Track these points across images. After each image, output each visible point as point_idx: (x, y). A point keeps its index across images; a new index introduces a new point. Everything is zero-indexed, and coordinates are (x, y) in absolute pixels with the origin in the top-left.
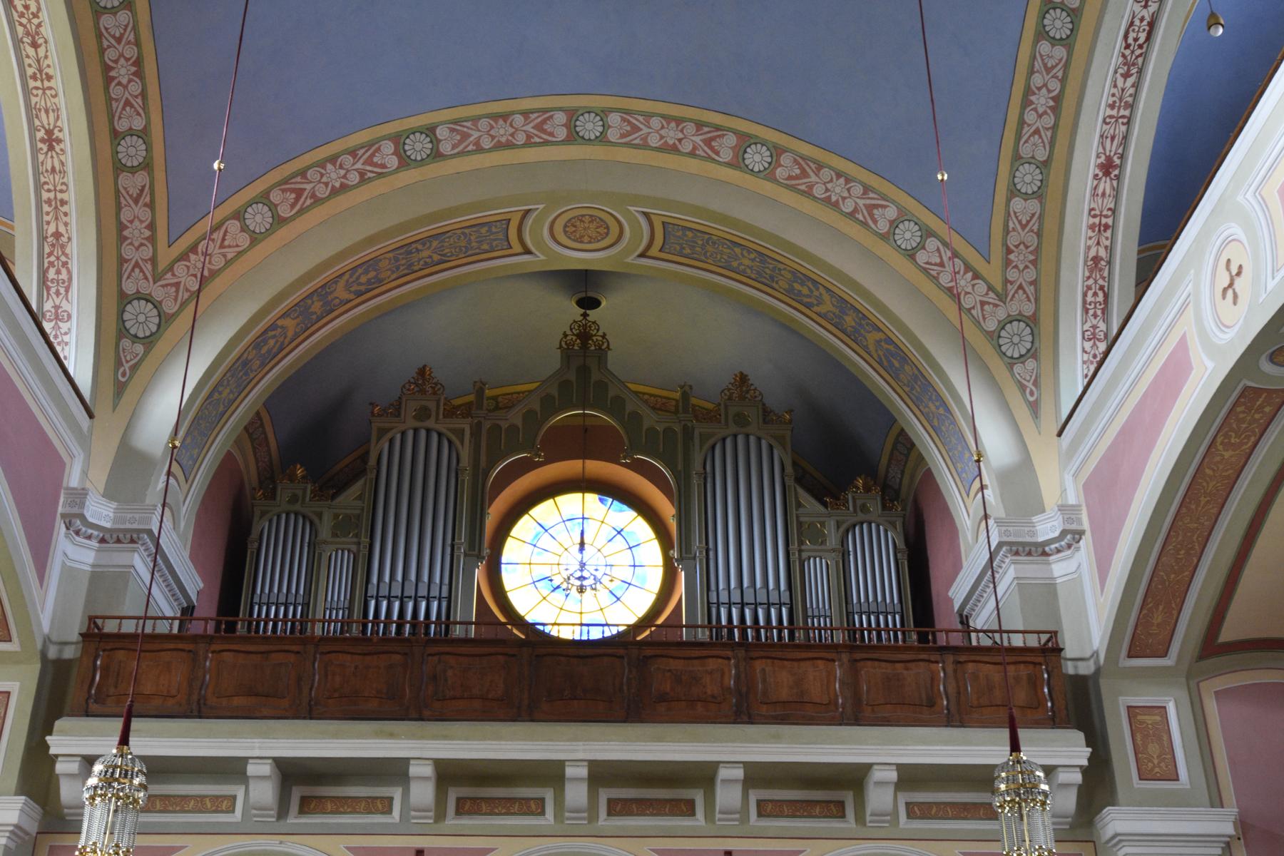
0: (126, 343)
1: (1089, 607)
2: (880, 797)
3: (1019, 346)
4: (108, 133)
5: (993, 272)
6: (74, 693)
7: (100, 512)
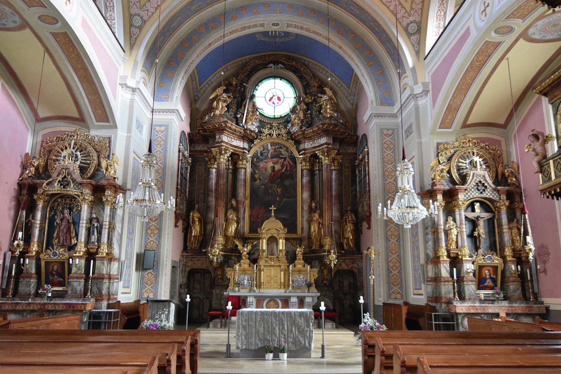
0: (133, 29)
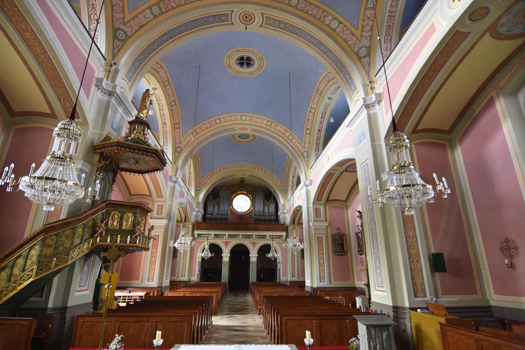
1: (288, 221)
2: (267, 237)
3: (285, 192)
4: (196, 172)
5: (283, 184)
6: (195, 228)
7: (196, 209)
